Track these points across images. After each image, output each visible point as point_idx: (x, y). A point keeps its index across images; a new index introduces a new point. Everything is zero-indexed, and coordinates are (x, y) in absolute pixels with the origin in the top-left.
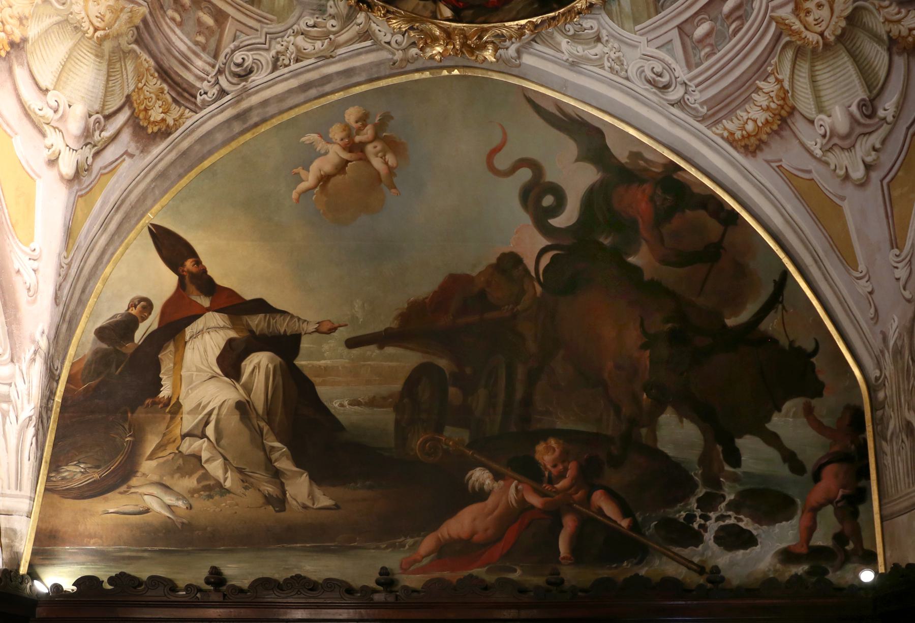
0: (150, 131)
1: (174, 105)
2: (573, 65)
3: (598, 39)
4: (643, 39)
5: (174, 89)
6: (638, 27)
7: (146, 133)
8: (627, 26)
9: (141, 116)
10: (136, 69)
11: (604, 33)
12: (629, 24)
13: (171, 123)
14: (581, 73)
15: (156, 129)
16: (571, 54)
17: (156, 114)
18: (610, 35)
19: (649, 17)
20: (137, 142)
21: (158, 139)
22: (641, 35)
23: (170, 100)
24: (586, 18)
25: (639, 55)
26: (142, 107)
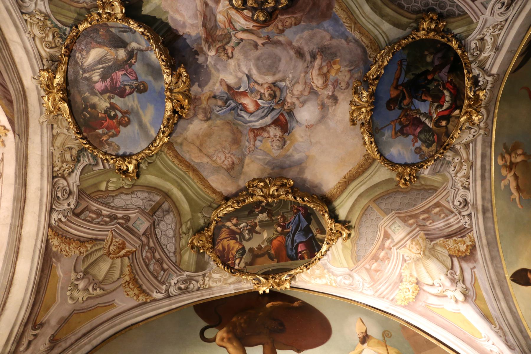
0: (468, 254)
1: (464, 239)
2: (497, 49)
3: (482, 39)
4: (481, 17)
5: (457, 235)
6: (475, 21)
7: (469, 256)
8: (474, 27)
9: (460, 254)
10: (441, 246)
11: (478, 37)
12: (473, 26)
13: (470, 243)
14: (503, 45)
15: (469, 251)
16: (491, 51)
17: (463, 248)
18: (479, 34)
19: (469, 17)
20: (470, 261)
21: (474, 252)
22: (479, 18)
23: (460, 239)
24: (470, 47)
25: (491, 17)
26: (457, 252)
